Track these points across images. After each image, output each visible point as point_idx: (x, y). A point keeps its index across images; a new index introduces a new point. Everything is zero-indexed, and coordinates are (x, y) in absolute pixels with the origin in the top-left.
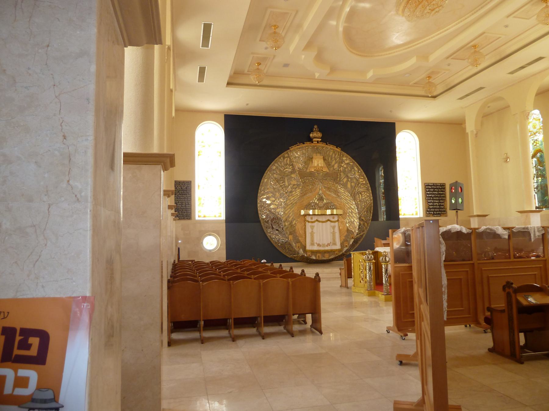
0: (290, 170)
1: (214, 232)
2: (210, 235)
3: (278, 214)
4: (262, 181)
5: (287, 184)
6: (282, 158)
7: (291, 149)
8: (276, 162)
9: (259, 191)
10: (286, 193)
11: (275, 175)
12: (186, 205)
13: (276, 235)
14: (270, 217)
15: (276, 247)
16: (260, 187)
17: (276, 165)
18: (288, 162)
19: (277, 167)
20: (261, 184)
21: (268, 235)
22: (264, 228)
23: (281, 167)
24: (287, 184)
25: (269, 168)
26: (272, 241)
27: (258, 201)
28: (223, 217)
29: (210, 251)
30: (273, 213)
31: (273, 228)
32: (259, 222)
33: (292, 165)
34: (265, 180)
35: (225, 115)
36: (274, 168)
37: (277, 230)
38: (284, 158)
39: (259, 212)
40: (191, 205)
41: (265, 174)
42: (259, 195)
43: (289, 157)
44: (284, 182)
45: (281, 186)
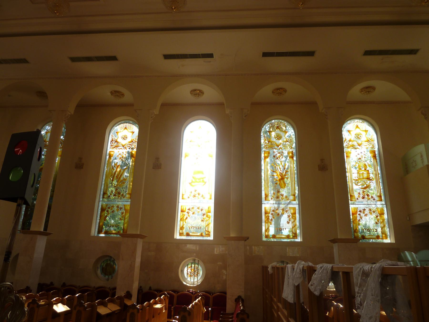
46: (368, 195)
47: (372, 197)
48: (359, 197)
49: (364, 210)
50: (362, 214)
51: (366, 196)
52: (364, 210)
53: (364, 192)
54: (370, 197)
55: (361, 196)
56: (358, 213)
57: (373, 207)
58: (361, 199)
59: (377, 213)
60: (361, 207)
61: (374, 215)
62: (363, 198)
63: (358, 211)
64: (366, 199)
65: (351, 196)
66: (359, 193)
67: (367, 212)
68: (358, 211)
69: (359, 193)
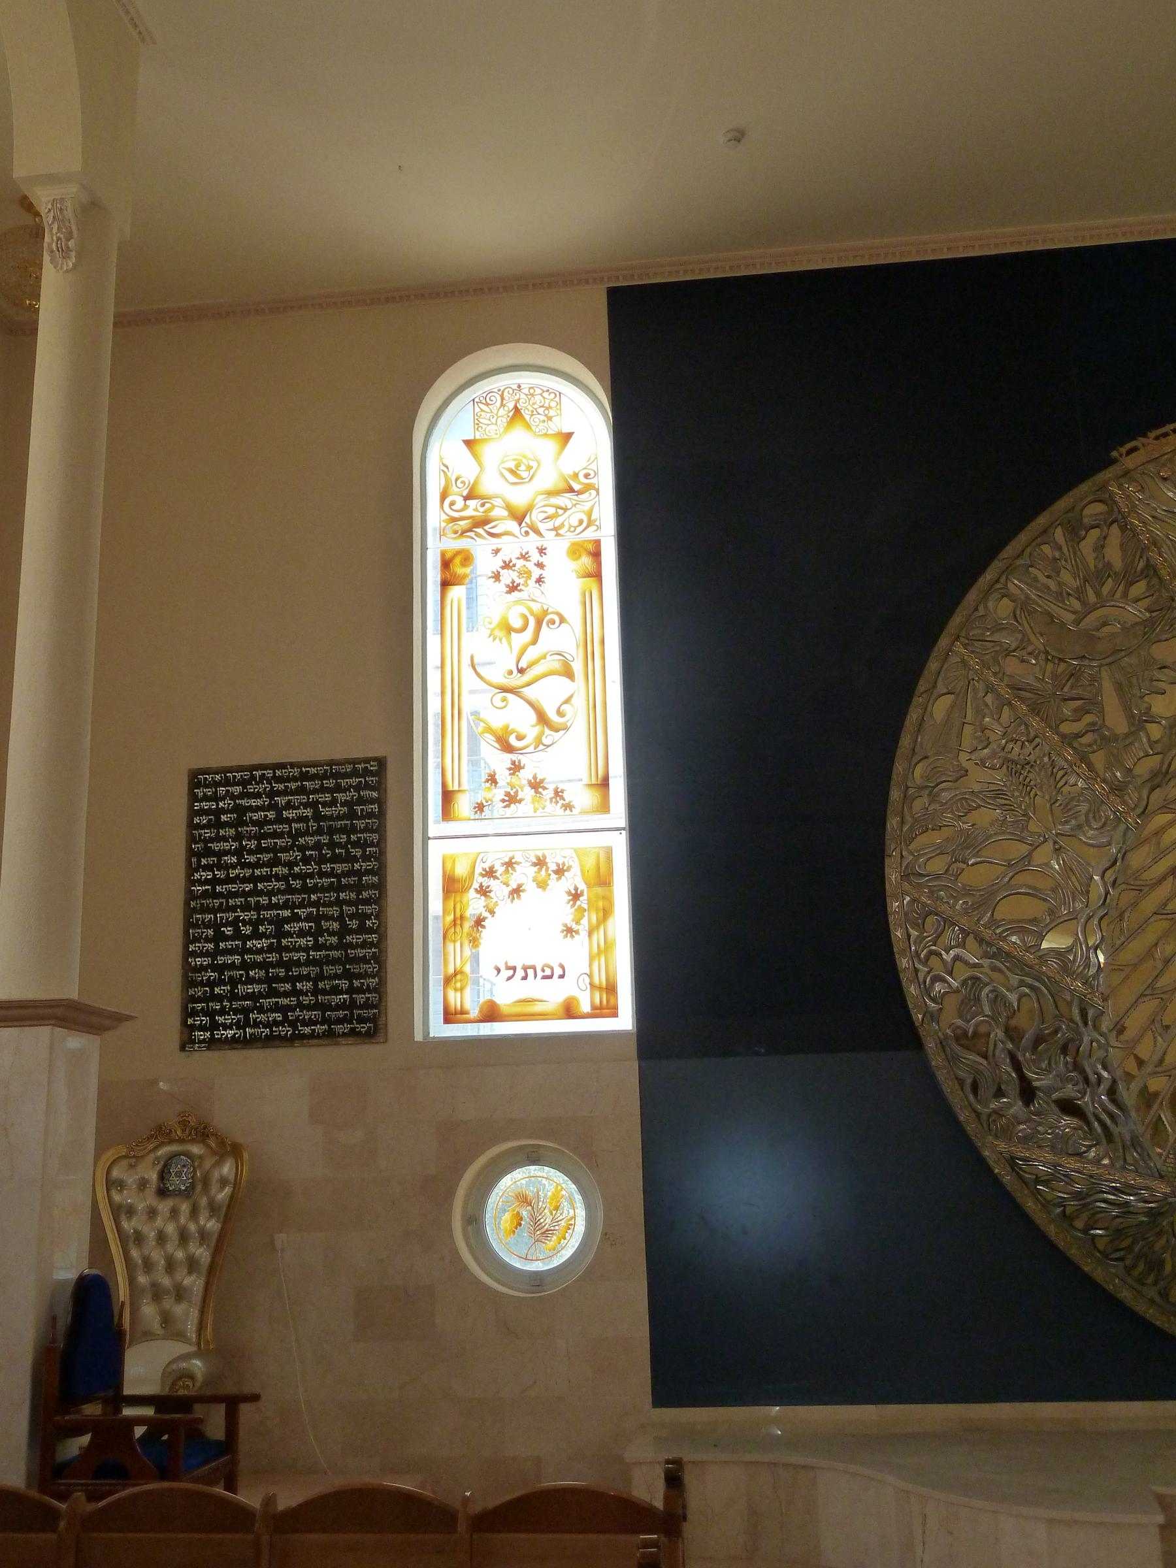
0: (1135, 612)
1: (549, 1128)
2: (534, 1157)
3: (1066, 969)
4: (913, 716)
5: (1117, 722)
6: (1059, 534)
7: (1130, 462)
8: (1008, 571)
9: (895, 794)
10: (1118, 789)
11: (1012, 666)
12: (344, 931)
13: (1061, 1146)
14: (997, 999)
15: (1073, 1252)
16: (899, 767)
17: (1015, 584)
18: (1114, 555)
19: (1024, 606)
20: (905, 741)
21: (993, 1150)
22: (948, 1087)
23: (1060, 596)
24: (1117, 722)
25: (957, 619)
26: (1030, 1205)
27: (892, 876)
28: (625, 1020)
29: (538, 1280)
30: (1020, 966)
31: (1028, 1093)
32: (911, 1039)
33: (1150, 571)
34: (933, 709)
35: (616, 296)
36: (1006, 606)
37: (1068, 1107)
38: (1075, 531)
39: (903, 963)
40: (381, 931)
41: (933, 665)
42: (892, 822)
43: (1116, 518)
44: (1092, 704)
45: (1069, 740)
46: (536, 785)
47: (558, 793)
49: (510, 864)
50: (498, 889)
51: (527, 793)
52: (510, 864)
53: (516, 768)
54: (548, 794)
56: (476, 885)
57: (558, 849)
59: (574, 879)
60: (494, 852)
61: (559, 889)
63: (478, 870)
67: (524, 874)
68: (478, 870)
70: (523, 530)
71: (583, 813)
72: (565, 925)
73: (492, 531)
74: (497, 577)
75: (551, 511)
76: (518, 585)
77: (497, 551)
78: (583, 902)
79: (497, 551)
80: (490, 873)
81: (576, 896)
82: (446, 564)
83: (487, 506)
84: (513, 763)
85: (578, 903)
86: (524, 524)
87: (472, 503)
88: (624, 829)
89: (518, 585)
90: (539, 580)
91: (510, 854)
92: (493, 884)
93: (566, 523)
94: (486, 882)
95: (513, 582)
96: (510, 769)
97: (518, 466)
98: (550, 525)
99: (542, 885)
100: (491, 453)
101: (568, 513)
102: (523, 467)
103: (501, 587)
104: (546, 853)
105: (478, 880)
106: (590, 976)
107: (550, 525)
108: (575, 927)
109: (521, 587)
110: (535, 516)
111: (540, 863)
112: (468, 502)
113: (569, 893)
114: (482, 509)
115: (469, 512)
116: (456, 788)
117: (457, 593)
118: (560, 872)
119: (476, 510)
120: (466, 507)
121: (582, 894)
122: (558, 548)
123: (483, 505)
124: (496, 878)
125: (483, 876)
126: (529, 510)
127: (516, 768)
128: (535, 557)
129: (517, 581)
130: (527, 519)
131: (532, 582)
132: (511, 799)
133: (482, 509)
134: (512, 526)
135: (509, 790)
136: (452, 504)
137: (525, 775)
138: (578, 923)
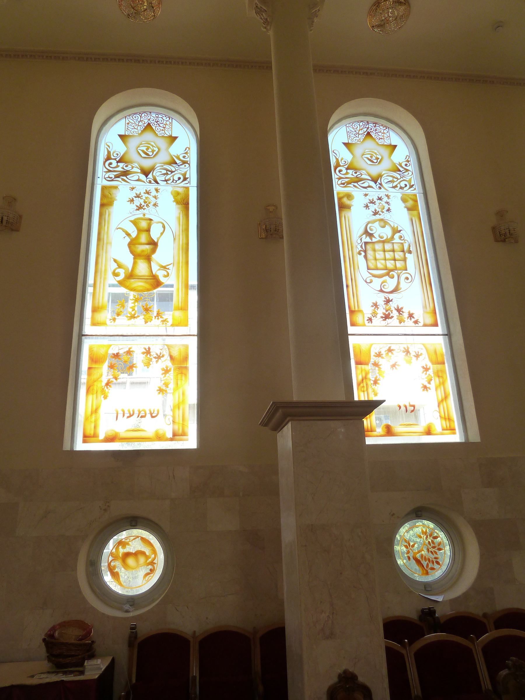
46: (399, 310)
47: (411, 316)
48: (375, 314)
51: (395, 313)
53: (388, 301)
54: (406, 315)
55: (381, 312)
56: (372, 361)
58: (378, 321)
62: (387, 317)
64: (394, 321)
65: (352, 312)
66: (375, 305)
67: (398, 356)
68: (373, 354)
69: (375, 305)
70: (378, 186)
71: (425, 325)
72: (423, 384)
73: (361, 185)
74: (367, 206)
75: (390, 179)
76: (378, 212)
77: (366, 195)
78: (430, 372)
79: (366, 195)
80: (379, 355)
81: (426, 369)
82: (340, 199)
83: (358, 173)
84: (386, 298)
85: (428, 373)
86: (377, 184)
87: (350, 171)
88: (447, 335)
89: (378, 212)
90: (388, 210)
91: (389, 345)
92: (380, 361)
93: (399, 185)
94: (377, 360)
95: (376, 210)
96: (385, 301)
97: (371, 157)
98: (391, 185)
99: (409, 362)
100: (358, 151)
101: (399, 181)
102: (374, 158)
103: (370, 212)
104: (409, 346)
105: (373, 359)
106: (439, 412)
107: (391, 185)
108: (428, 385)
109: (380, 213)
110: (384, 180)
111: (407, 352)
112: (348, 171)
113: (423, 367)
114: (355, 175)
115: (349, 176)
116: (356, 309)
117: (345, 213)
118: (417, 356)
119: (352, 175)
120: (347, 173)
121: (429, 369)
122: (396, 197)
123: (356, 173)
124: (382, 358)
125: (376, 356)
126: (380, 176)
127: (388, 301)
128: (385, 199)
129: (378, 210)
130: (379, 181)
131: (385, 210)
132: (387, 317)
133: (355, 175)
134: (372, 184)
135: (384, 311)
136: (340, 171)
137: (392, 306)
138: (429, 383)
